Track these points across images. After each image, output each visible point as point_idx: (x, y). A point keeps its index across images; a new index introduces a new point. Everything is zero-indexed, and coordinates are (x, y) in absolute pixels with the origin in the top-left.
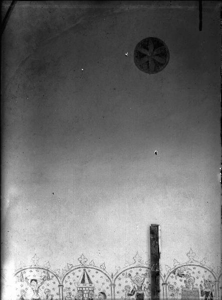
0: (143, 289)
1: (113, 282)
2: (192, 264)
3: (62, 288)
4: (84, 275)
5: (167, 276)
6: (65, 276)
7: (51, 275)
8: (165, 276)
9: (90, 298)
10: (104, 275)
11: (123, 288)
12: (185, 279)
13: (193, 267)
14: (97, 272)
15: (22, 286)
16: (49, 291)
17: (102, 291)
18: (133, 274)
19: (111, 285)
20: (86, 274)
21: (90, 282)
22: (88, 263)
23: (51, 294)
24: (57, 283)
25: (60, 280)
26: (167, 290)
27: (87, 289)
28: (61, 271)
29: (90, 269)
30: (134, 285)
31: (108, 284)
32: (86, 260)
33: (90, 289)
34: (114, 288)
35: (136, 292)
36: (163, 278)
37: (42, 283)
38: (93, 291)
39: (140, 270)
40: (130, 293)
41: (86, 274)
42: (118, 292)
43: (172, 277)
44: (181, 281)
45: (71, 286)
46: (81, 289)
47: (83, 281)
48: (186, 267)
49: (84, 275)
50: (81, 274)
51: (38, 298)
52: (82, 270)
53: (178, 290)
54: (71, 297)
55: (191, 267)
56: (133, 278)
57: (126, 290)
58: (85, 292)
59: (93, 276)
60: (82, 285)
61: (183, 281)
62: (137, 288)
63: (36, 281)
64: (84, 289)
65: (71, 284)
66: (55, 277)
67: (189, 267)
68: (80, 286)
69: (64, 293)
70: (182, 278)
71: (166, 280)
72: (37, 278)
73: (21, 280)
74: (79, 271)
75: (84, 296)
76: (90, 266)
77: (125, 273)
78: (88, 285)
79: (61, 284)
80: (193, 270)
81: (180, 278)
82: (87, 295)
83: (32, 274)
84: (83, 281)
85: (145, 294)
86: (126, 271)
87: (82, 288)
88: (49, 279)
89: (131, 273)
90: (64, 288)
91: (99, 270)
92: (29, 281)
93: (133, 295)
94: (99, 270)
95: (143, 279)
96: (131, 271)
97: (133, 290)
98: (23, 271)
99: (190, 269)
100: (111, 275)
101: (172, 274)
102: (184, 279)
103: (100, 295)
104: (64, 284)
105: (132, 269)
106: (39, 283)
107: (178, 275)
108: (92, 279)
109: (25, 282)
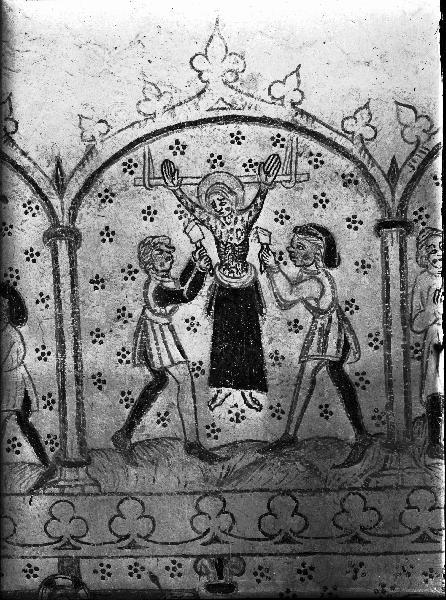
0: (252, 257)
1: (64, 220)
5: (408, 174)
18: (192, 166)
19: (50, 237)
30: (196, 233)
34: (72, 252)
35: (209, 281)
36: (384, 186)
39: (237, 139)
42: (97, 281)
56: (189, 190)
85: (267, 294)
89: (177, 160)
93: (191, 297)
95: (251, 193)
96: (180, 148)
97: (190, 266)
105: (182, 136)
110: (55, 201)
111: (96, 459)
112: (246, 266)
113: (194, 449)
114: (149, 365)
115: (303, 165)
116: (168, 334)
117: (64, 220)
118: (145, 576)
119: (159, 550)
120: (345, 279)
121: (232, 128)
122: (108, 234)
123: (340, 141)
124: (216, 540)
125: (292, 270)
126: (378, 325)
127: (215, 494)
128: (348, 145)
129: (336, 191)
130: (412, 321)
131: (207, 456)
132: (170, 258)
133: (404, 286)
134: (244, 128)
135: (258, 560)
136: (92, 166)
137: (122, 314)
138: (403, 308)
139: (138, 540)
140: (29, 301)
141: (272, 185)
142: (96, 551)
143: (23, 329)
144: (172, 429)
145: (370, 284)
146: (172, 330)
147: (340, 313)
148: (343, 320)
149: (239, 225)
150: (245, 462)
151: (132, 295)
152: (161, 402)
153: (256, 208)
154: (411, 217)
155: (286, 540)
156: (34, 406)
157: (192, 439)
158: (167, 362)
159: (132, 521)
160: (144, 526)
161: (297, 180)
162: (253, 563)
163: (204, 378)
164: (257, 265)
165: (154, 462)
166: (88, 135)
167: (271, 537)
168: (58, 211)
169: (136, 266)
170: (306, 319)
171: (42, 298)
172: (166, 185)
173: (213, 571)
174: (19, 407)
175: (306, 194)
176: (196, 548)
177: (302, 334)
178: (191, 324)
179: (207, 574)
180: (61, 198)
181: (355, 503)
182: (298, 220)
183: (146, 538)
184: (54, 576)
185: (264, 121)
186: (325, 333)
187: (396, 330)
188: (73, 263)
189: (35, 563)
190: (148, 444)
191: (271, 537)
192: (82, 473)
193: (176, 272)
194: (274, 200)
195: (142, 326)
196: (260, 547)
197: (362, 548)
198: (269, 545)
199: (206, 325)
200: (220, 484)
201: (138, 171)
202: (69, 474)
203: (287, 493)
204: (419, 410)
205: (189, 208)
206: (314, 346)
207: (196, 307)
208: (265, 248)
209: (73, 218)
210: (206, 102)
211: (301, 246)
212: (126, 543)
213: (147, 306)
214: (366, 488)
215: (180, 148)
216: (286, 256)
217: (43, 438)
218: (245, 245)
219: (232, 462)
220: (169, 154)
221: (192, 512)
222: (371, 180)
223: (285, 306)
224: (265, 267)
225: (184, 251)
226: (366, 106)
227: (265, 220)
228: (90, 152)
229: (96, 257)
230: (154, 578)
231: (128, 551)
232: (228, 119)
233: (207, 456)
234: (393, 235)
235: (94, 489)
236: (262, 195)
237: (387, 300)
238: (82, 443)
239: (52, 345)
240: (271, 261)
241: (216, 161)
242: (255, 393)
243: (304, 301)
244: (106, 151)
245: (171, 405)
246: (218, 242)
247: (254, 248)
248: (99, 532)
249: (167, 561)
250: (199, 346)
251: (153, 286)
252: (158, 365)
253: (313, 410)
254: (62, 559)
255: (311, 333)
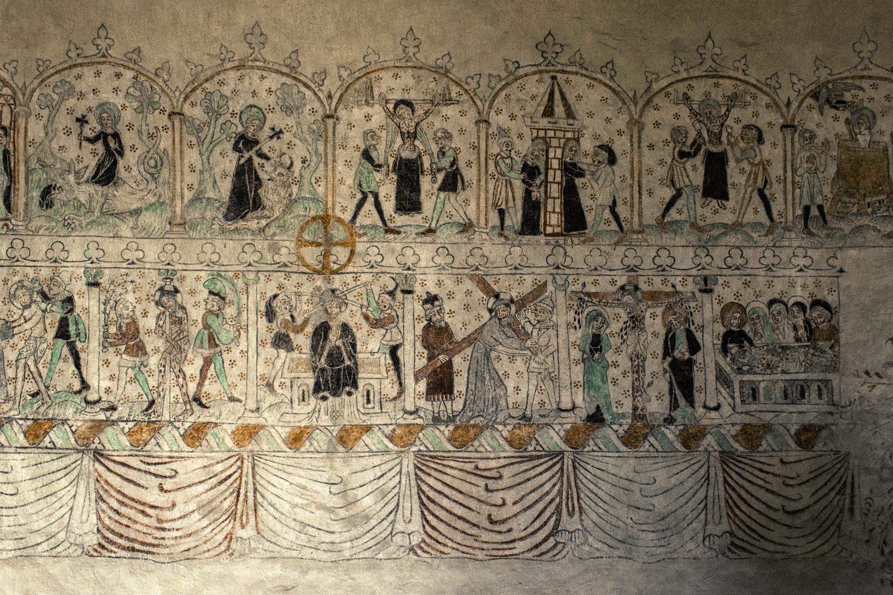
0: (724, 138)
1: (636, 117)
2: (866, 73)
3: (487, 129)
4: (552, 94)
6: (496, 95)
7: (455, 90)
8: (789, 104)
9: (568, 160)
10: (607, 93)
11: (665, 134)
12: (847, 114)
13: (871, 82)
14: (590, 86)
15: (368, 118)
16: (448, 136)
17: (605, 139)
18: (697, 96)
20: (557, 95)
21: (570, 114)
22: (563, 59)
23: (453, 146)
24: (472, 114)
25: (481, 107)
26: (797, 145)
27: (560, 134)
28: (484, 82)
29: (571, 77)
30: (698, 126)
31: (621, 122)
32: (558, 49)
33: (569, 135)
34: (639, 132)
35: (703, 148)
36: (784, 110)
37: (427, 113)
38: (577, 140)
39: (717, 85)
40: (686, 149)
41: (557, 95)
42: (651, 147)
43: (810, 108)
44: (836, 119)
45: (512, 125)
46: (542, 134)
47: (549, 112)
48: (849, 81)
49: (552, 94)
50: (542, 90)
51: (414, 156)
52: (547, 77)
53: (826, 143)
54: (513, 154)
55: (865, 84)
56: (695, 107)
57: (675, 141)
58: (554, 143)
59: (579, 97)
60: (544, 122)
61: (842, 120)
62: (705, 135)
63: (408, 104)
64: (551, 134)
65: (512, 117)
66: (465, 97)
67: (857, 82)
68: (537, 125)
69: (490, 141)
70: (839, 113)
71: (794, 115)
72: (412, 96)
73: (366, 101)
74: (540, 81)
75: (551, 155)
76: (569, 69)
77: (670, 89)
78: (562, 124)
79: (485, 117)
80: (872, 93)
81: (833, 112)
82: (559, 152)
83: (398, 84)
84: (549, 112)
85: (730, 155)
86: (675, 86)
87: (545, 130)
88: (448, 101)
89: (690, 93)
90: (493, 129)
91: (595, 79)
92: (391, 106)
93: (695, 154)
94: (595, 79)
95: (723, 110)
96: (690, 87)
97: (695, 141)
98: (373, 75)
99: (861, 89)
100: (631, 94)
101: (809, 101)
102: (844, 115)
103: (596, 154)
104: (494, 118)
105: (694, 83)
106: (420, 112)
107: (828, 101)
108: (580, 109)
109: (378, 108)
110: (632, 108)
111: (647, 230)
112: (721, 143)
113: (694, 225)
114: (674, 186)
115: (748, 98)
116: (683, 171)
117: (636, 117)
118: (669, 284)
119: (679, 273)
120: (766, 151)
121: (715, 80)
122: (657, 124)
123: (765, 88)
124: (704, 268)
125: (742, 145)
126: (781, 172)
127: (704, 247)
128: (768, 90)
129: (762, 111)
130: (796, 171)
131: (700, 230)
132: (686, 137)
133: (793, 154)
134: (721, 81)
135: (725, 278)
136: (649, 95)
137: (662, 162)
138: (792, 165)
139: (668, 268)
140: (618, 153)
141: (733, 106)
142: (646, 273)
143: (615, 167)
144: (684, 217)
145: (779, 151)
146: (685, 170)
147: (763, 165)
148: (765, 169)
149: (718, 123)
150: (717, 233)
151: (667, 153)
152: (679, 203)
153: (726, 116)
154: (796, 123)
155: (737, 268)
156: (618, 203)
157: (692, 220)
158: (682, 185)
159: (664, 260)
160: (669, 261)
161: (745, 105)
162: (721, 280)
163: (700, 194)
164: (726, 142)
165: (675, 232)
166: (649, 80)
167: (730, 267)
168: (634, 113)
169: (669, 139)
170: (748, 168)
171: (624, 153)
172: (684, 104)
173: (702, 282)
174: (611, 204)
175: (750, 110)
176: (694, 272)
177: (746, 175)
178: (694, 168)
179: (699, 284)
180: (636, 107)
181: (769, 253)
182: (745, 122)
183: (670, 267)
184: (625, 285)
185: (729, 78)
186: (756, 175)
187: (789, 174)
188: (640, 137)
189: (616, 278)
190: (672, 223)
191: (730, 267)
192: (640, 236)
193: (690, 141)
194: (735, 113)
195: (671, 168)
196: (725, 272)
197: (772, 273)
198: (730, 272)
199: (701, 169)
200: (706, 243)
201: (672, 97)
202: (635, 237)
203: (738, 247)
204: (799, 212)
205: (694, 114)
206: (751, 181)
207: (699, 160)
208: (729, 134)
209: (641, 116)
210: (704, 68)
211: (746, 134)
212: (660, 269)
213: (674, 159)
214: (774, 246)
215: (690, 87)
216: (739, 138)
217: (622, 218)
218: (721, 133)
219: (712, 233)
220: (686, 90)
221: (693, 255)
222: (778, 106)
223: (738, 161)
224: (729, 143)
225: (692, 135)
226: (776, 74)
227: (730, 122)
228: (648, 89)
229: (651, 134)
230: (673, 286)
231: (661, 273)
232: (713, 77)
233: (700, 230)
234: (788, 131)
235: (646, 244)
236: (728, 110)
237: (785, 160)
238: (640, 224)
239: (628, 175)
240: (733, 140)
241: (707, 94)
242: (724, 202)
243: (747, 159)
244: (656, 87)
245: (684, 205)
246: (708, 131)
247: (725, 134)
248: (647, 264)
249: (680, 278)
250: (698, 177)
251: (677, 149)
252: (678, 186)
253: (750, 210)
254: (629, 276)
255: (750, 175)
